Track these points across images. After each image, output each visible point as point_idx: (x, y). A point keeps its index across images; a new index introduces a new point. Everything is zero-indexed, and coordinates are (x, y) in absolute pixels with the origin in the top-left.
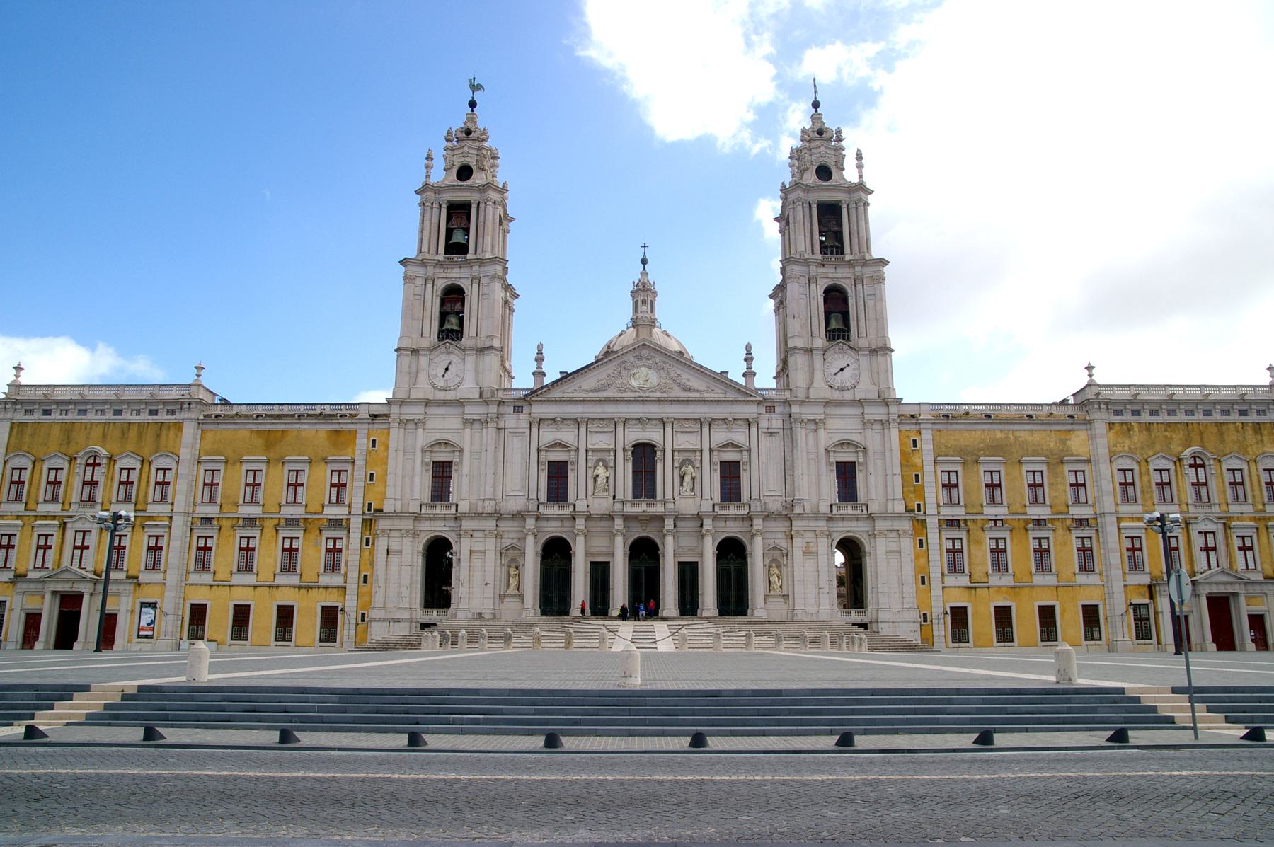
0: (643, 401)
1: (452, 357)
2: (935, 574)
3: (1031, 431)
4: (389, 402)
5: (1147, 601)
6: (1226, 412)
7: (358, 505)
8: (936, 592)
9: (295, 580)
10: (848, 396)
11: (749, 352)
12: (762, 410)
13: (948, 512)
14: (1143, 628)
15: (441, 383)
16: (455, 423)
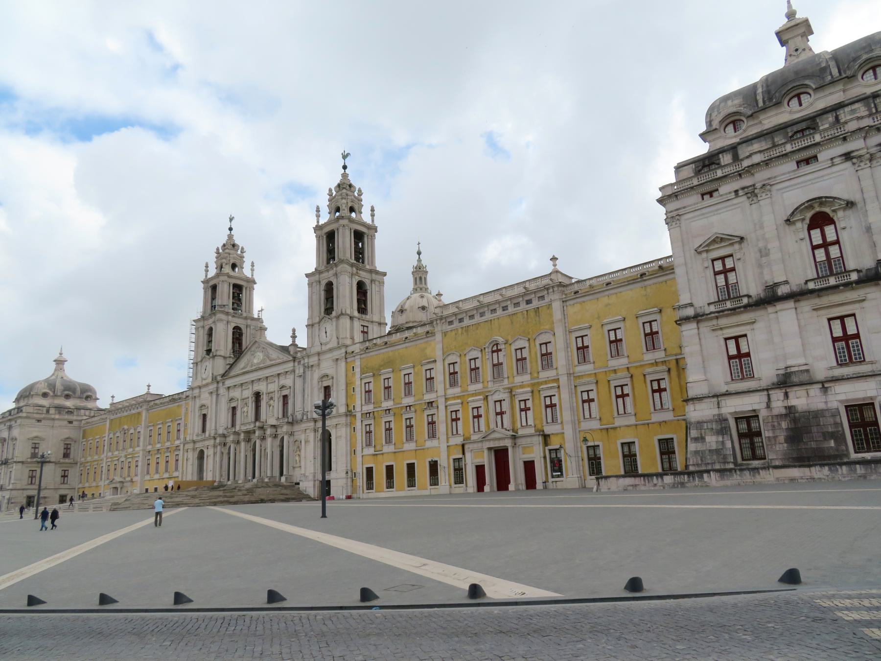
0: (261, 369)
1: (207, 363)
2: (359, 449)
3: (406, 348)
4: (191, 389)
5: (460, 456)
6: (517, 305)
7: (182, 440)
8: (359, 459)
9: (166, 475)
10: (328, 347)
11: (294, 334)
12: (296, 364)
13: (366, 409)
14: (459, 476)
15: (204, 377)
16: (207, 395)
